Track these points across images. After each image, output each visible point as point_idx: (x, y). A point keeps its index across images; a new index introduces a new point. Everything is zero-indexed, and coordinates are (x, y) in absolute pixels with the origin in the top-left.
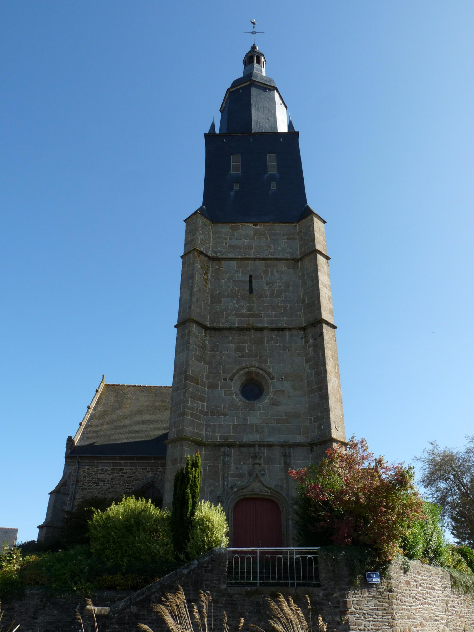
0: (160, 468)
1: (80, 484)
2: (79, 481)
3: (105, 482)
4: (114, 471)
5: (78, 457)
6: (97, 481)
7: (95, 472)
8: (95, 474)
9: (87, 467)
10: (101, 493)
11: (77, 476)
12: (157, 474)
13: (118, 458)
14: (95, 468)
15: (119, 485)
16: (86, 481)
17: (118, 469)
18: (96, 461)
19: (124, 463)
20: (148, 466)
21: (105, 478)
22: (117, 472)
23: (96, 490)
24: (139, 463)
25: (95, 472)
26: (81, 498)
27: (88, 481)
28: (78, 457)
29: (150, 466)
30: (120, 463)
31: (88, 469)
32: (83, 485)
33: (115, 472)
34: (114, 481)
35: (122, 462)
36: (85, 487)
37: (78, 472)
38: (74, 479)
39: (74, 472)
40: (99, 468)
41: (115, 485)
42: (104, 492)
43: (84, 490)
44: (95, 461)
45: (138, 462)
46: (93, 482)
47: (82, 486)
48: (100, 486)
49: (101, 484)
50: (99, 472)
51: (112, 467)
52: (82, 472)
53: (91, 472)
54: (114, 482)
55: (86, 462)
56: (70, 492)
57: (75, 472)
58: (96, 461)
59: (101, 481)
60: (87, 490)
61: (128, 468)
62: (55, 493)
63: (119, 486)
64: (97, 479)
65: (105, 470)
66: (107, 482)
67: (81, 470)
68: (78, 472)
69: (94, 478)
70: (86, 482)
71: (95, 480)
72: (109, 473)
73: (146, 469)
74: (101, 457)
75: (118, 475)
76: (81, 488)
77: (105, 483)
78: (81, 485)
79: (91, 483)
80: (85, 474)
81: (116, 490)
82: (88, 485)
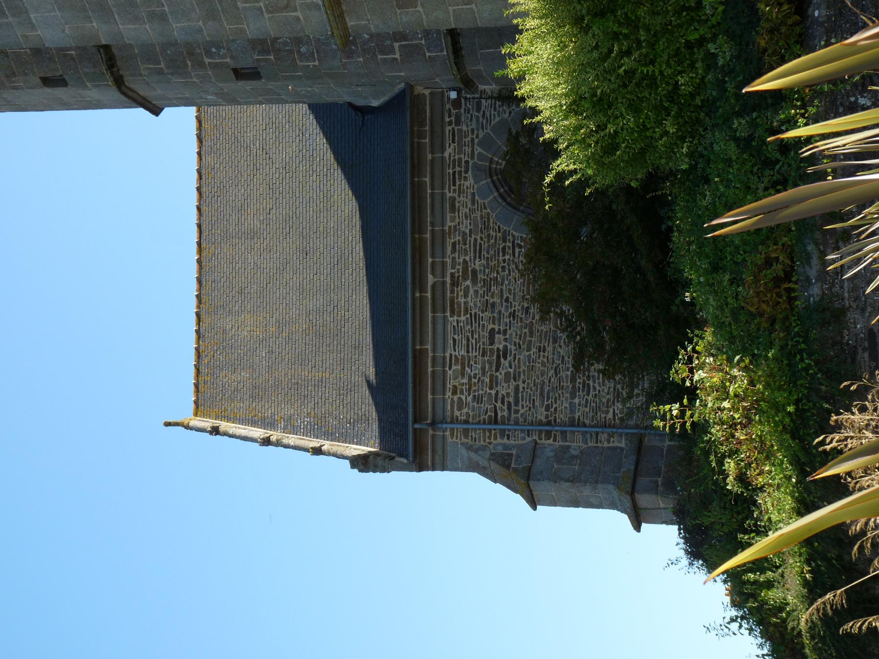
0: (446, 155)
1: (502, 410)
2: (493, 414)
3: (493, 329)
4: (459, 305)
5: (416, 426)
6: (491, 355)
7: (463, 368)
8: (470, 366)
9: (450, 394)
10: (528, 338)
11: (479, 423)
12: (467, 162)
13: (418, 295)
14: (450, 369)
15: (502, 285)
16: (493, 392)
17: (452, 292)
18: (430, 364)
19: (433, 274)
20: (443, 195)
21: (481, 333)
22: (462, 293)
23: (522, 357)
24: (433, 224)
25: (463, 368)
26: (546, 403)
27: (491, 388)
28: (416, 426)
29: (443, 188)
30: (434, 286)
31: (454, 392)
32: (506, 399)
33: (463, 300)
34: (492, 300)
35: (431, 279)
36: (512, 394)
37: (466, 422)
38: (487, 434)
39: (466, 437)
40: (451, 355)
41: (502, 296)
42: (527, 330)
43: (520, 395)
44: (430, 369)
45: (429, 228)
46: (494, 369)
47: (509, 403)
48: (506, 346)
49: (499, 344)
50: (463, 352)
51: (448, 314)
52: (465, 410)
53: (465, 381)
54: (495, 300)
55: (434, 400)
56: (528, 439)
57: (466, 432)
58: (430, 364)
59: (492, 343)
60: (521, 385)
61: (448, 260)
62: (531, 483)
63: (506, 282)
64: (486, 359)
65: (456, 337)
66: (494, 323)
67: (457, 413)
68: (466, 422)
69: (483, 369)
70: (497, 394)
71: (490, 363)
72: (467, 319)
73: (453, 200)
74: (414, 350)
75: (471, 291)
76: (513, 407)
77: (496, 327)
78: (505, 407)
79: (500, 377)
80: (470, 399)
81: (517, 290)
82: (506, 385)
